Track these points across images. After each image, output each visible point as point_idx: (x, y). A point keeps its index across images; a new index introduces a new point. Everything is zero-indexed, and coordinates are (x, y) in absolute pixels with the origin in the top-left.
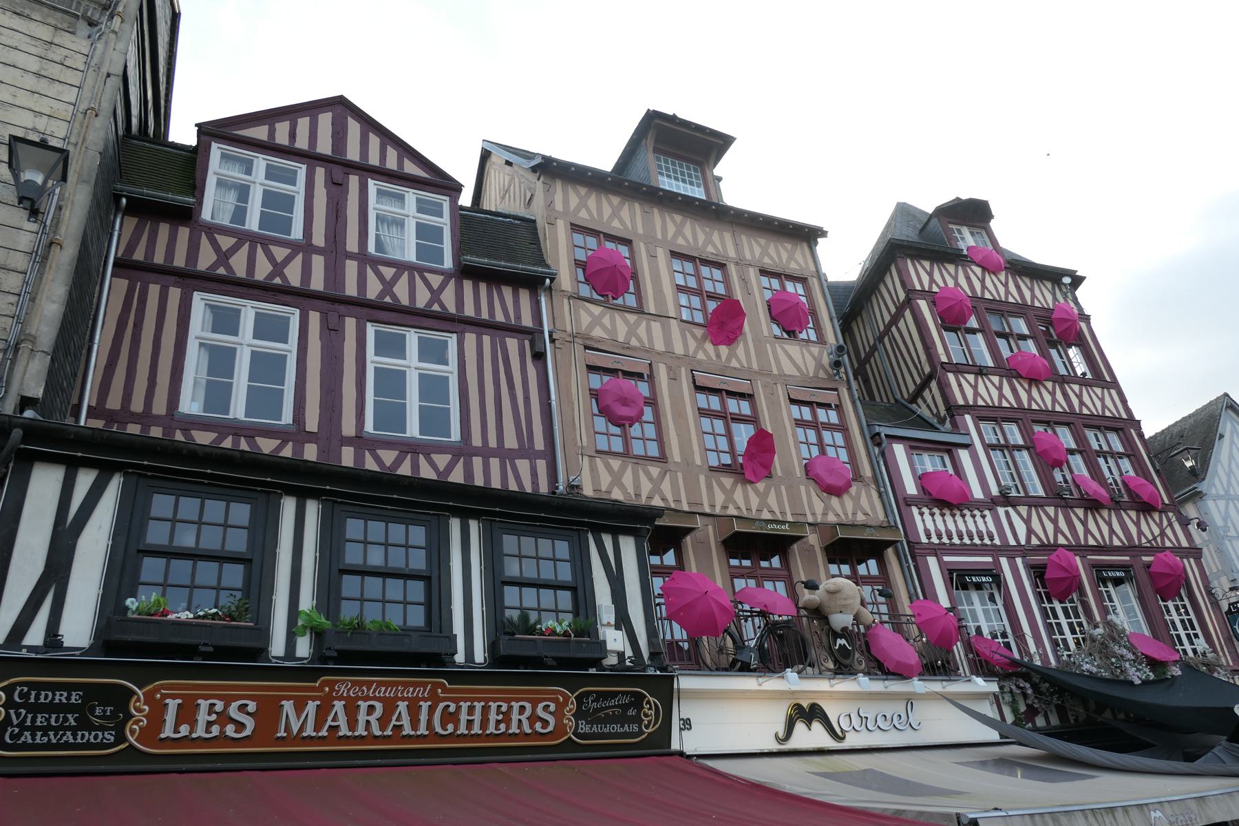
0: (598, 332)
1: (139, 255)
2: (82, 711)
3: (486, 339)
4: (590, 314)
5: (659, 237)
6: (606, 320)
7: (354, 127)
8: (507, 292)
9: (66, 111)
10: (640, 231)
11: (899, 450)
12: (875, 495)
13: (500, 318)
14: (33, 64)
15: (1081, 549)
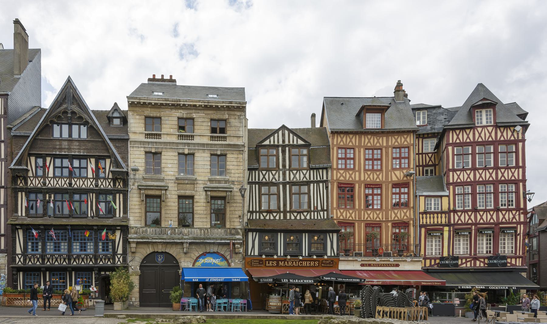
0: (342, 178)
1: (250, 180)
2: (259, 263)
3: (315, 184)
4: (340, 173)
5: (363, 145)
6: (344, 175)
7: (286, 132)
8: (321, 171)
9: (242, 171)
10: (357, 144)
11: (422, 199)
12: (412, 211)
13: (319, 179)
14: (235, 163)
15: (476, 224)
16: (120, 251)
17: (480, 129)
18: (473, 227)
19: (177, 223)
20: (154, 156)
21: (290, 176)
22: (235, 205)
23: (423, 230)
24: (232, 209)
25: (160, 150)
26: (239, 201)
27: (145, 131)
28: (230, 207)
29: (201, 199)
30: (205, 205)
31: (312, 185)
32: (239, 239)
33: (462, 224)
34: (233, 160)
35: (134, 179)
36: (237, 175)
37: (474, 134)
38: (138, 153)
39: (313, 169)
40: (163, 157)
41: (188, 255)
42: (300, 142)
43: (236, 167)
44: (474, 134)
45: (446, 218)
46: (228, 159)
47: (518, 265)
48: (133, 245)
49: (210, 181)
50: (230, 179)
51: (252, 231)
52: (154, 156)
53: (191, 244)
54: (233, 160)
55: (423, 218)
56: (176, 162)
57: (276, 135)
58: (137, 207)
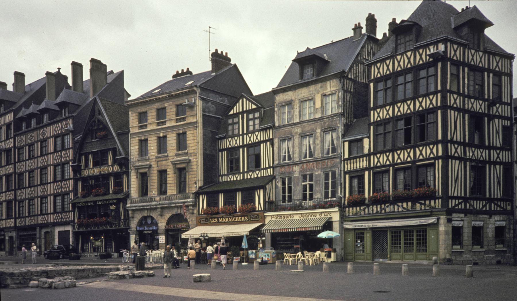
7: (245, 100)
14: (192, 138)
16: (122, 218)
17: (399, 57)
18: (391, 168)
19: (156, 193)
20: (143, 143)
21: (247, 140)
22: (192, 173)
23: (347, 176)
24: (190, 176)
25: (146, 137)
26: (194, 169)
27: (140, 123)
28: (189, 175)
29: (170, 172)
30: (173, 176)
31: (262, 145)
32: (189, 202)
33: (381, 166)
34: (190, 135)
35: (133, 162)
36: (193, 148)
37: (394, 63)
38: (135, 141)
39: (262, 130)
40: (149, 142)
41: (163, 217)
42: (254, 107)
43: (193, 141)
44: (394, 63)
45: (366, 161)
46: (188, 136)
47: (437, 207)
48: (130, 212)
49: (176, 155)
50: (189, 152)
51: (202, 194)
52: (143, 143)
53: (162, 208)
54: (190, 135)
55: (347, 164)
56: (156, 144)
57: (238, 104)
58: (135, 183)
